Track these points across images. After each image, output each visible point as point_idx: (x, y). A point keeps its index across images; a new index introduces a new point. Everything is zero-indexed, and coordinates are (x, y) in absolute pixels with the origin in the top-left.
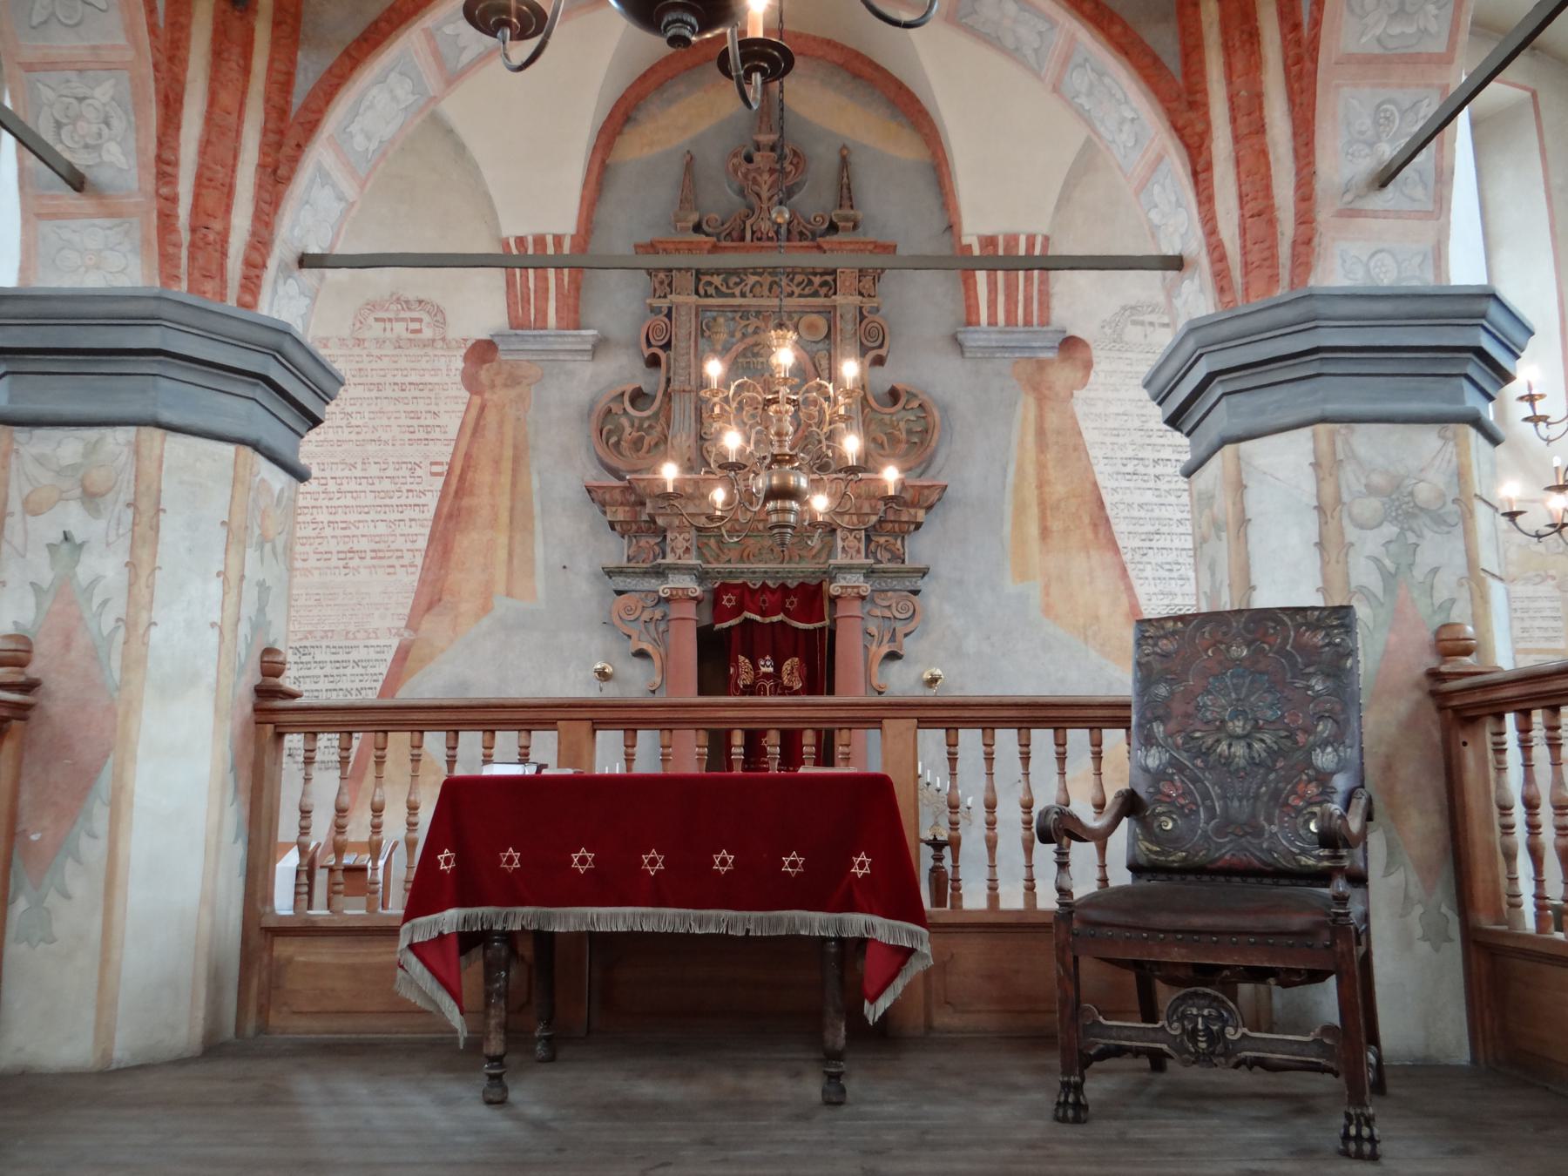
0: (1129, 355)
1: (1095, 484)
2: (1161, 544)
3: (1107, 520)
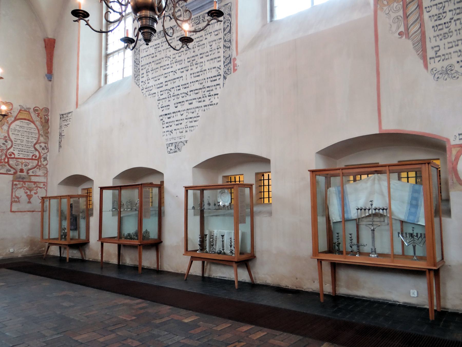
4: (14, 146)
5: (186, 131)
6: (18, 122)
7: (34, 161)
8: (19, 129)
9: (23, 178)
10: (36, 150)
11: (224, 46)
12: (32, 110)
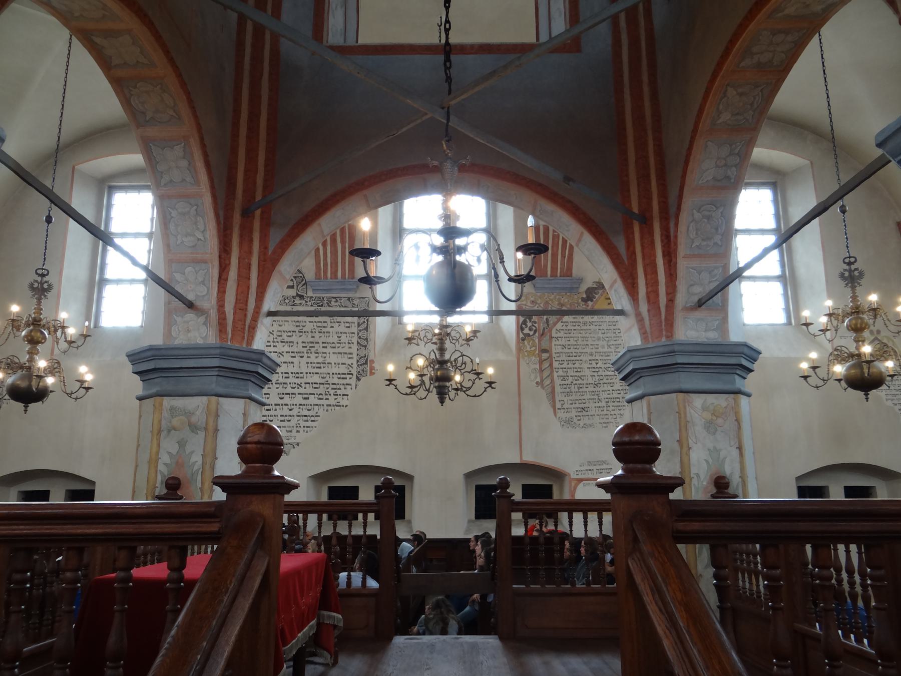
5: (298, 431)
11: (358, 343)
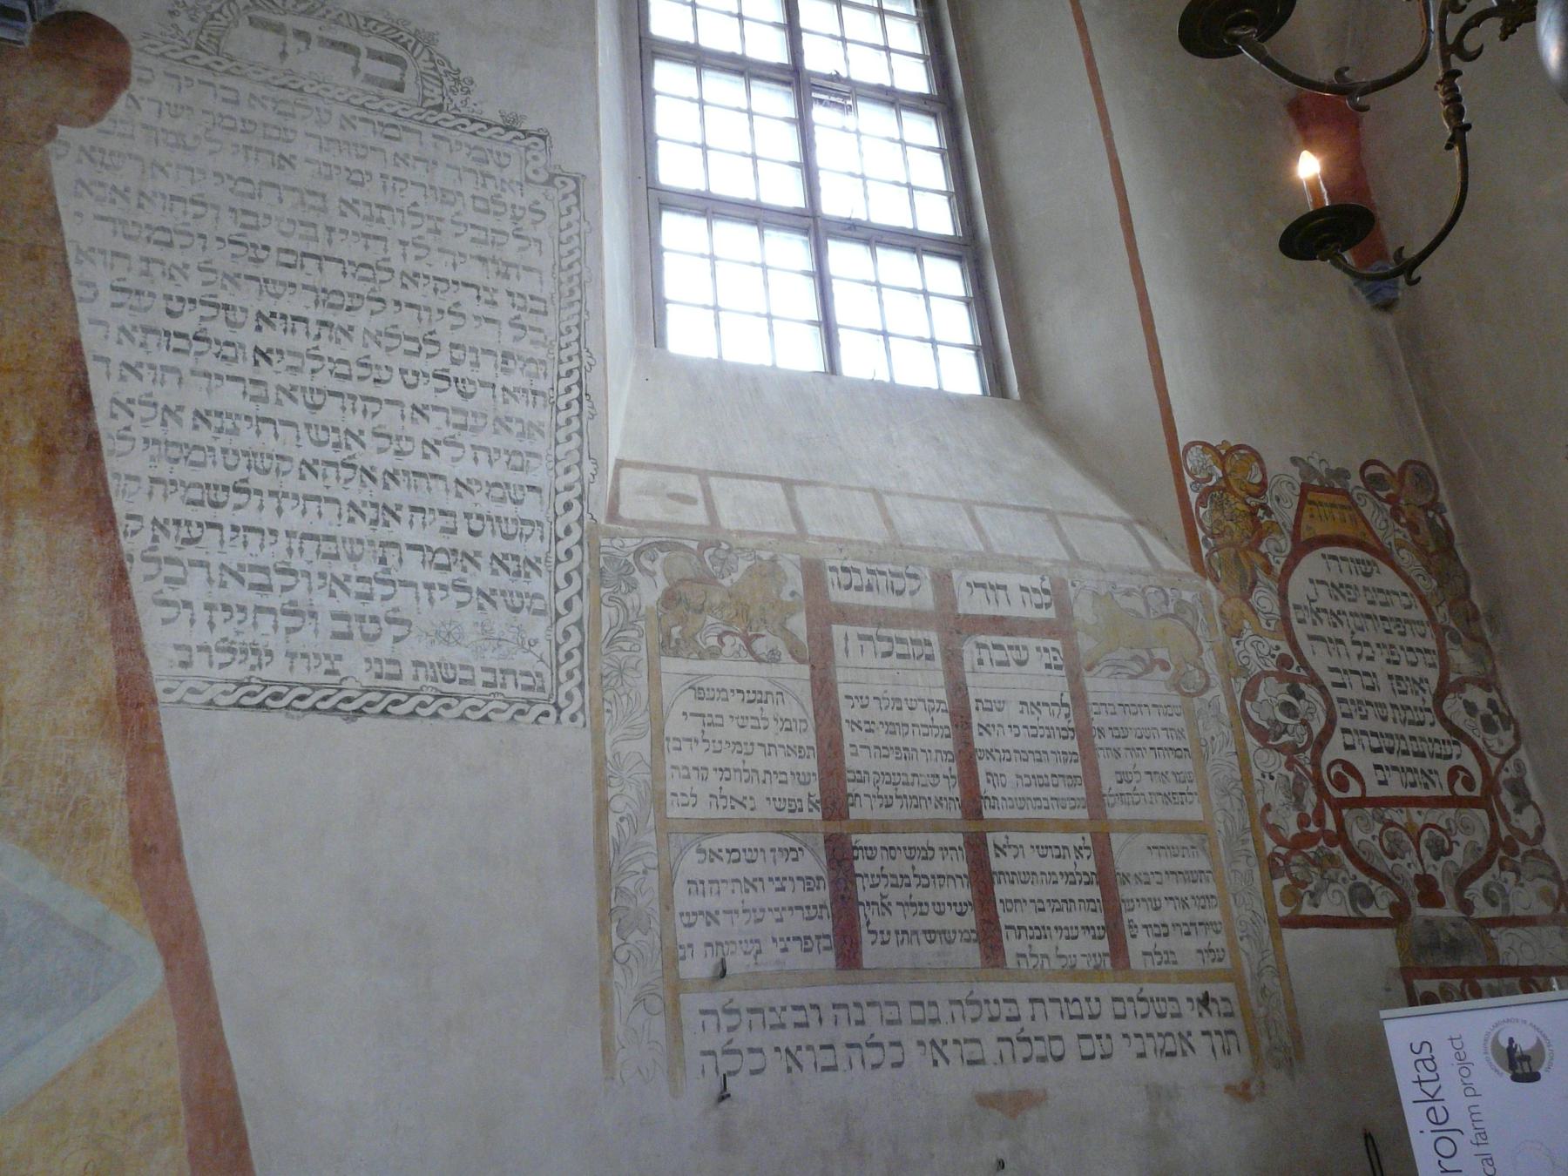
0: (229, 81)
1: (74, 348)
2: (245, 517)
3: (93, 441)
4: (1342, 722)
6: (1312, 564)
7: (1468, 814)
8: (1335, 606)
9: (1455, 947)
10: (1458, 735)
12: (1355, 481)
